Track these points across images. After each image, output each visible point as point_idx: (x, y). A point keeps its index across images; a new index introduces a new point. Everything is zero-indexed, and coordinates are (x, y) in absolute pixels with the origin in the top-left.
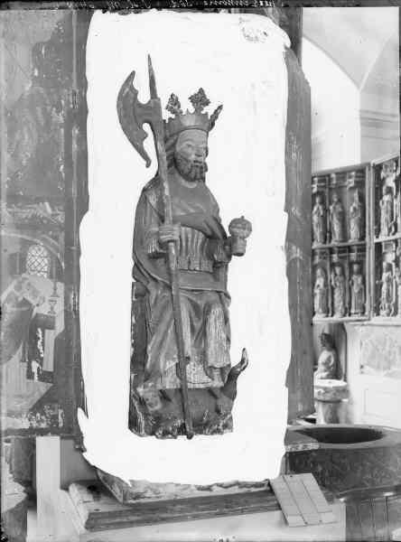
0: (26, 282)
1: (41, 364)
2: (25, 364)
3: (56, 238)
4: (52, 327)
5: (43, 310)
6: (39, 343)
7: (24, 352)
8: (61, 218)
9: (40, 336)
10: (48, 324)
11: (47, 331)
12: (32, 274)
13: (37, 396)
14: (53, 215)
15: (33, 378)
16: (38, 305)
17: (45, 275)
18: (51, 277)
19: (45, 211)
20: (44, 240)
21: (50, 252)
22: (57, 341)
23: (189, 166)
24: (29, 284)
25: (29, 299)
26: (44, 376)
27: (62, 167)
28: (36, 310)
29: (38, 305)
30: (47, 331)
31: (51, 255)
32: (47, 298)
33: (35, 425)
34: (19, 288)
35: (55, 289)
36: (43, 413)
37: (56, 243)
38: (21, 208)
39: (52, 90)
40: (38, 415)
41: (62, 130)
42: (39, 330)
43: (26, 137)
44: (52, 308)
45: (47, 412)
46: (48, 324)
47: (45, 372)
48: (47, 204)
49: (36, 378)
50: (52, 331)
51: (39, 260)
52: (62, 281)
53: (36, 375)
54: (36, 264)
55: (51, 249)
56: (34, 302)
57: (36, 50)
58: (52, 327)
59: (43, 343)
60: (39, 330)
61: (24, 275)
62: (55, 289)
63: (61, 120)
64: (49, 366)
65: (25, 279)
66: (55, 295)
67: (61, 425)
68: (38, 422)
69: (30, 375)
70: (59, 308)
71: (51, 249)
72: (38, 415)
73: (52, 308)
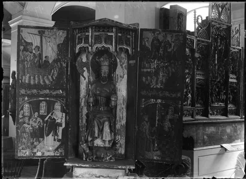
0: (54, 113)
1: (58, 136)
2: (53, 137)
3: (63, 100)
4: (61, 126)
5: (59, 121)
6: (58, 130)
7: (53, 133)
8: (64, 94)
9: (58, 128)
10: (60, 125)
11: (60, 127)
12: (56, 110)
13: (56, 146)
14: (62, 93)
15: (56, 141)
16: (57, 120)
17: (60, 111)
18: (61, 111)
19: (60, 92)
20: (60, 101)
21: (61, 104)
22: (63, 130)
23: (102, 78)
24: (55, 114)
25: (55, 118)
26: (59, 140)
27: (65, 79)
28: (57, 121)
29: (57, 120)
30: (60, 127)
31: (61, 105)
32: (60, 117)
33: (56, 154)
34: (52, 114)
35: (62, 115)
36: (58, 151)
37: (63, 102)
38: (53, 92)
39: (63, 57)
40: (57, 151)
41: (65, 69)
42: (58, 127)
43: (55, 71)
44: (61, 121)
45: (59, 151)
46: (60, 125)
47: (60, 139)
48: (61, 91)
49: (56, 141)
50: (61, 127)
51: (58, 106)
52: (64, 113)
53: (56, 140)
54: (57, 108)
55: (62, 103)
56: (56, 119)
57: (58, 46)
58: (61, 126)
59: (59, 131)
60: (58, 127)
61: (53, 111)
62: (62, 115)
63: (65, 66)
64: (60, 137)
65: (54, 112)
66: (62, 117)
67: (63, 155)
68: (57, 153)
69: (55, 140)
70: (64, 120)
71: (62, 103)
72: (57, 151)
73: (61, 121)
